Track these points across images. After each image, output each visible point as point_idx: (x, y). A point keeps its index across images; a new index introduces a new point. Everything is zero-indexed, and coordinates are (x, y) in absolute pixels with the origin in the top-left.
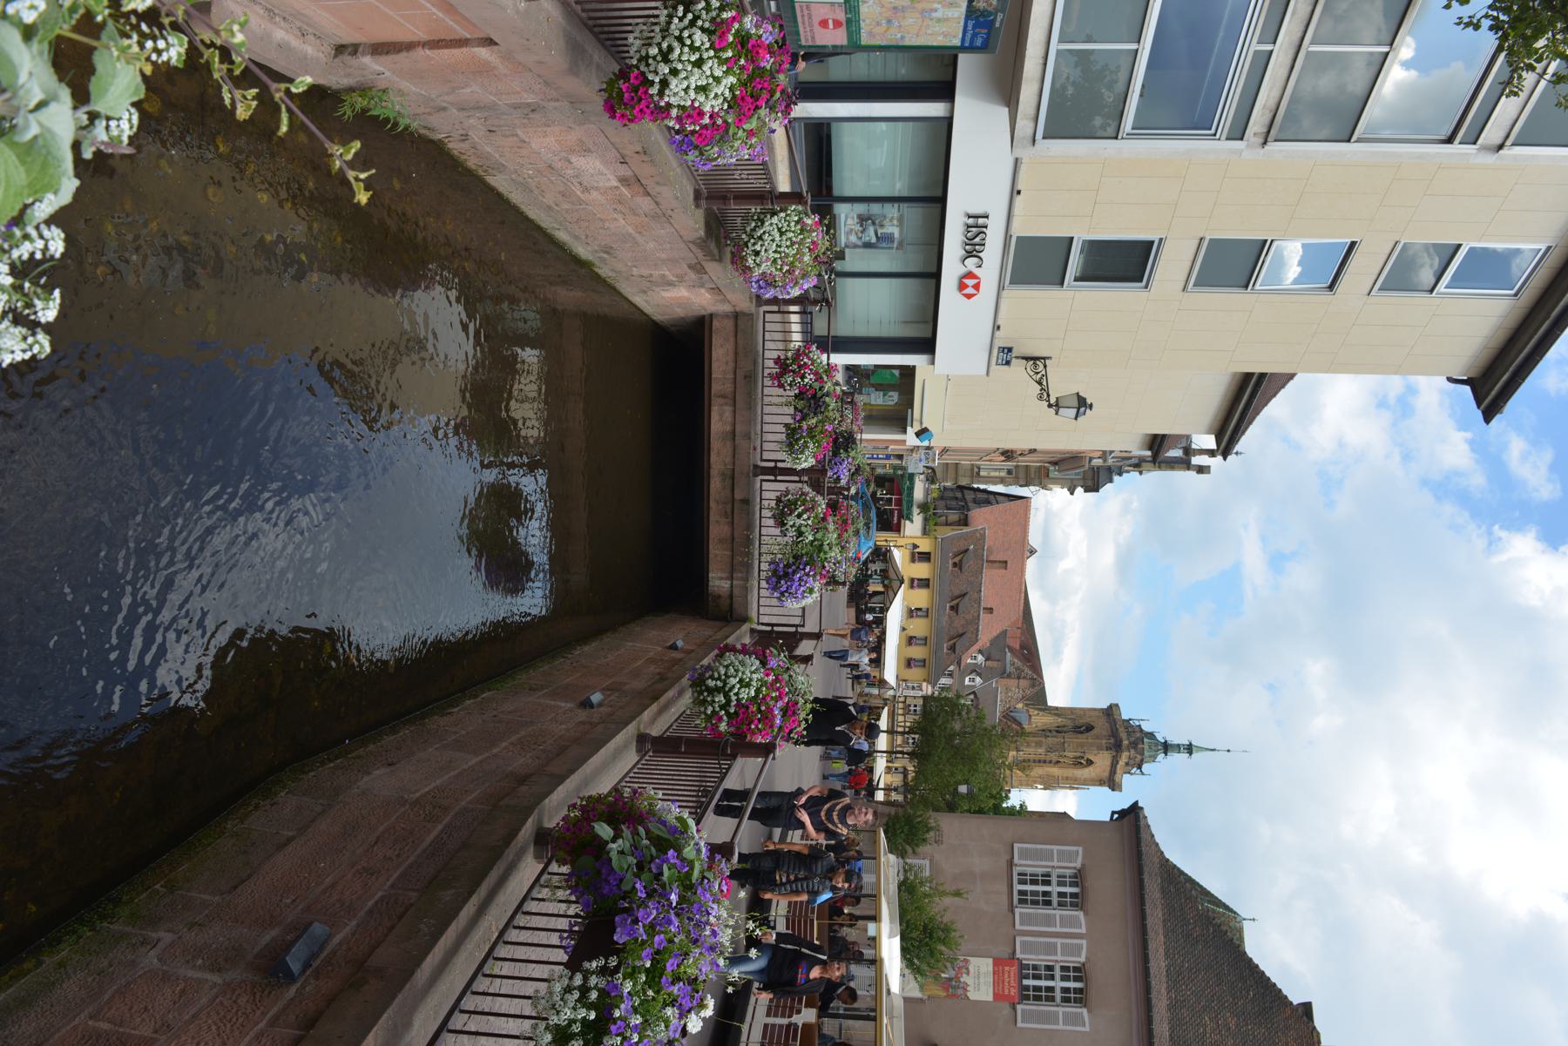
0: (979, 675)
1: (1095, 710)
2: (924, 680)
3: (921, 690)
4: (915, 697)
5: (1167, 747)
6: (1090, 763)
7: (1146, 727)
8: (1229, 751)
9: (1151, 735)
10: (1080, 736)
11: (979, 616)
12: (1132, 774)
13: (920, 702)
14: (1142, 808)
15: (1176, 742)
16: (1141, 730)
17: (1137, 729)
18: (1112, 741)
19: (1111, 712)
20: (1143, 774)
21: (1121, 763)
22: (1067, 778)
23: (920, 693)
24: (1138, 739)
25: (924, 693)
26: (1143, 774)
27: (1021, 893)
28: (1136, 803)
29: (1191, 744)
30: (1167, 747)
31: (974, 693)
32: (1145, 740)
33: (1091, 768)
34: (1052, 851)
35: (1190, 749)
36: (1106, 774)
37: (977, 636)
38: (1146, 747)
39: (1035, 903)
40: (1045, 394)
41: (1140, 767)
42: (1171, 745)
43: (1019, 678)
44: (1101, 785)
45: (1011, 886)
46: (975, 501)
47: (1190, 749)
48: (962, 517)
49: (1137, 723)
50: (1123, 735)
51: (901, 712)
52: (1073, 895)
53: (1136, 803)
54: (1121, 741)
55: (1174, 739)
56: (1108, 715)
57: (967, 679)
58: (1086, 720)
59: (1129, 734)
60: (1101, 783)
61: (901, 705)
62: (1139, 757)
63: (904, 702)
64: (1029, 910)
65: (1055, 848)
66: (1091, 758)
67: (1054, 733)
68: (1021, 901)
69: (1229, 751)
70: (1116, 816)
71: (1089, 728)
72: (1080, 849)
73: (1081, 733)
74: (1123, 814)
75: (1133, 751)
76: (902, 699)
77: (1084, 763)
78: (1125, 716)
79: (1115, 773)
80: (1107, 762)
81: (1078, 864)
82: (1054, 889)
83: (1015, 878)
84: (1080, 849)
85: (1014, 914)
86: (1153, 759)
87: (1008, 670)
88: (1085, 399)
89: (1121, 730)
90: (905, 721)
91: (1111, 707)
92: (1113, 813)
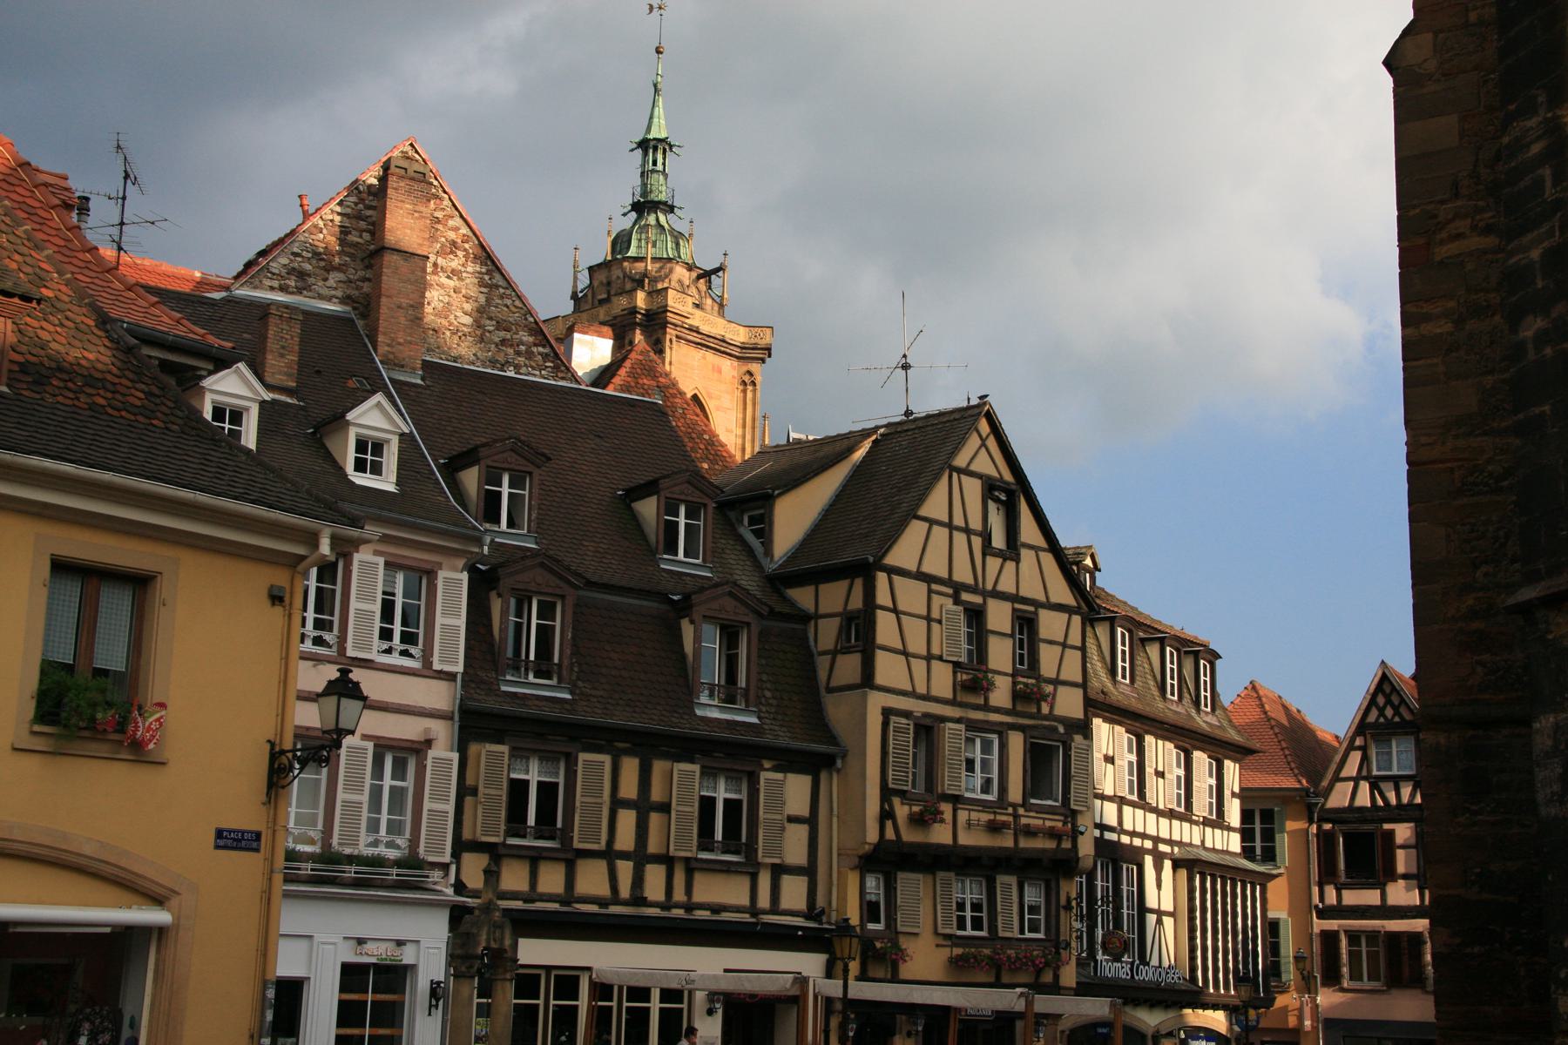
0: (337, 421)
3: (419, 748)
4: (465, 791)
9: (621, 242)
15: (639, 182)
16: (605, 265)
17: (601, 276)
21: (697, 319)
23: (443, 752)
25: (442, 733)
32: (632, 252)
42: (644, 193)
49: (584, 280)
51: (552, 880)
61: (514, 878)
63: (496, 854)
90: (610, 855)
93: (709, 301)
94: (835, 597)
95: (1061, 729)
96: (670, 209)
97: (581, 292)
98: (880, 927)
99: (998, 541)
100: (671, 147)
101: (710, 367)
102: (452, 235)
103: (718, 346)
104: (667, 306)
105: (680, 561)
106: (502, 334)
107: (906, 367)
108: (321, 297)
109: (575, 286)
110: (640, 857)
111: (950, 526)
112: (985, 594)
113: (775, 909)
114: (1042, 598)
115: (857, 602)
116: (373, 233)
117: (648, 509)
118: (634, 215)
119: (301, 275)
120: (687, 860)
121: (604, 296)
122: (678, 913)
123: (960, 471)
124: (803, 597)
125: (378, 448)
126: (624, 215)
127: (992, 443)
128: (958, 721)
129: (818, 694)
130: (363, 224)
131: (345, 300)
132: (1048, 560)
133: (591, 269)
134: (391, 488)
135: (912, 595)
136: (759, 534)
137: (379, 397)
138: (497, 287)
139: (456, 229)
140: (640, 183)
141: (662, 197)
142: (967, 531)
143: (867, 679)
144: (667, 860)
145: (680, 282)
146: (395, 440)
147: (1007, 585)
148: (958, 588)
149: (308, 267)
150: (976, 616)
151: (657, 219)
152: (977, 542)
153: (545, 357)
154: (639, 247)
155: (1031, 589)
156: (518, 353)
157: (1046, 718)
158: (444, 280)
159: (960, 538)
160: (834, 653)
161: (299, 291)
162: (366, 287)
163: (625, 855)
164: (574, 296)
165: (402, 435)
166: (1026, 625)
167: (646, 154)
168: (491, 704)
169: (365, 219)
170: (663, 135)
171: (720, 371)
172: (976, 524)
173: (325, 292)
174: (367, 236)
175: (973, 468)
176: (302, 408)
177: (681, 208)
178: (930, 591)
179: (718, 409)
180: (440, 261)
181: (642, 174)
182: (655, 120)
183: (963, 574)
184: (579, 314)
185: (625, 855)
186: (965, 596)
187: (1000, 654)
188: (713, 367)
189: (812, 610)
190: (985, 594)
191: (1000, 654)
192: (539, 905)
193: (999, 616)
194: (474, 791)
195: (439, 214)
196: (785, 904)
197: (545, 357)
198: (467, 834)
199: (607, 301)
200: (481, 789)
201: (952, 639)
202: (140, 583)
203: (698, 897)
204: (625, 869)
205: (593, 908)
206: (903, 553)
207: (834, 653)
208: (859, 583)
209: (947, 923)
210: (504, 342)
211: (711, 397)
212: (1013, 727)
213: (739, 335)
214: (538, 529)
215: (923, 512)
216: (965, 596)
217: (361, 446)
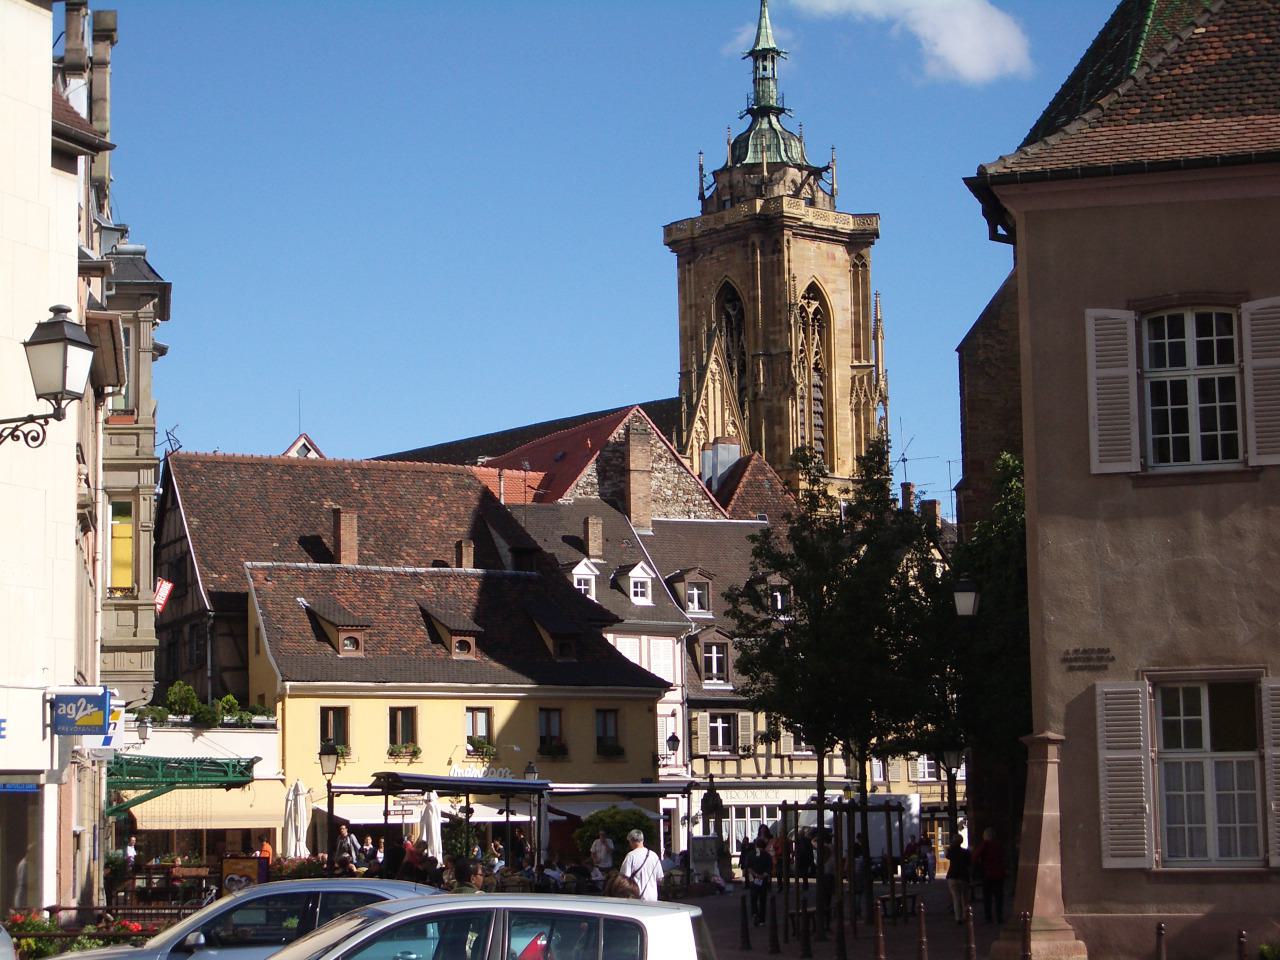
1: (682, 283)
6: (814, 292)
7: (720, 157)
9: (739, 147)
10: (749, 317)
13: (703, 717)
14: (982, 170)
15: (750, 88)
16: (725, 169)
17: (725, 179)
19: (684, 243)
21: (810, 216)
22: (857, 346)
27: (1209, 453)
28: (967, 181)
31: (670, 582)
32: (748, 160)
33: (828, 289)
34: (1101, 380)
38: (766, 158)
39: (1230, 417)
40: (27, 428)
41: (816, 173)
42: (757, 100)
45: (1196, 477)
49: (710, 179)
52: (1203, 326)
53: (967, 181)
54: (755, 217)
57: (638, 601)
59: (735, 200)
61: (715, 768)
62: (793, 173)
64: (1249, 430)
65: (1093, 374)
66: (801, 289)
67: (747, 380)
68: (1231, 452)
70: (1001, 231)
72: (1091, 313)
73: (741, 313)
74: (997, 216)
75: (779, 190)
76: (698, 765)
78: (694, 210)
79: (834, 232)
81: (1128, 317)
82: (1192, 373)
83: (1173, 467)
84: (1091, 313)
85: (1261, 468)
88: (41, 326)
91: (672, 244)
92: (994, 236)
93: (820, 194)
96: (779, 111)
97: (708, 189)
100: (778, 53)
101: (825, 255)
102: (659, 451)
103: (831, 235)
104: (783, 212)
106: (686, 497)
107: (904, 460)
109: (701, 187)
110: (768, 756)
113: (831, 774)
118: (749, 118)
120: (789, 756)
121: (728, 197)
122: (787, 779)
126: (741, 118)
130: (618, 454)
133: (715, 173)
134: (651, 604)
137: (642, 564)
138: (682, 473)
139: (661, 448)
140: (752, 91)
141: (773, 102)
144: (781, 757)
145: (793, 181)
146: (650, 584)
151: (770, 123)
154: (755, 152)
156: (694, 505)
158: (657, 474)
163: (762, 756)
164: (701, 196)
165: (652, 578)
167: (756, 60)
169: (618, 451)
170: (772, 45)
171: (834, 258)
177: (790, 110)
180: (655, 465)
181: (754, 81)
182: (763, 30)
184: (707, 217)
185: (762, 756)
188: (828, 255)
192: (727, 780)
194: (696, 733)
196: (835, 772)
197: (708, 504)
198: (694, 752)
200: (699, 733)
202: (615, 711)
203: (795, 772)
204: (762, 761)
205: (750, 779)
211: (826, 282)
213: (848, 225)
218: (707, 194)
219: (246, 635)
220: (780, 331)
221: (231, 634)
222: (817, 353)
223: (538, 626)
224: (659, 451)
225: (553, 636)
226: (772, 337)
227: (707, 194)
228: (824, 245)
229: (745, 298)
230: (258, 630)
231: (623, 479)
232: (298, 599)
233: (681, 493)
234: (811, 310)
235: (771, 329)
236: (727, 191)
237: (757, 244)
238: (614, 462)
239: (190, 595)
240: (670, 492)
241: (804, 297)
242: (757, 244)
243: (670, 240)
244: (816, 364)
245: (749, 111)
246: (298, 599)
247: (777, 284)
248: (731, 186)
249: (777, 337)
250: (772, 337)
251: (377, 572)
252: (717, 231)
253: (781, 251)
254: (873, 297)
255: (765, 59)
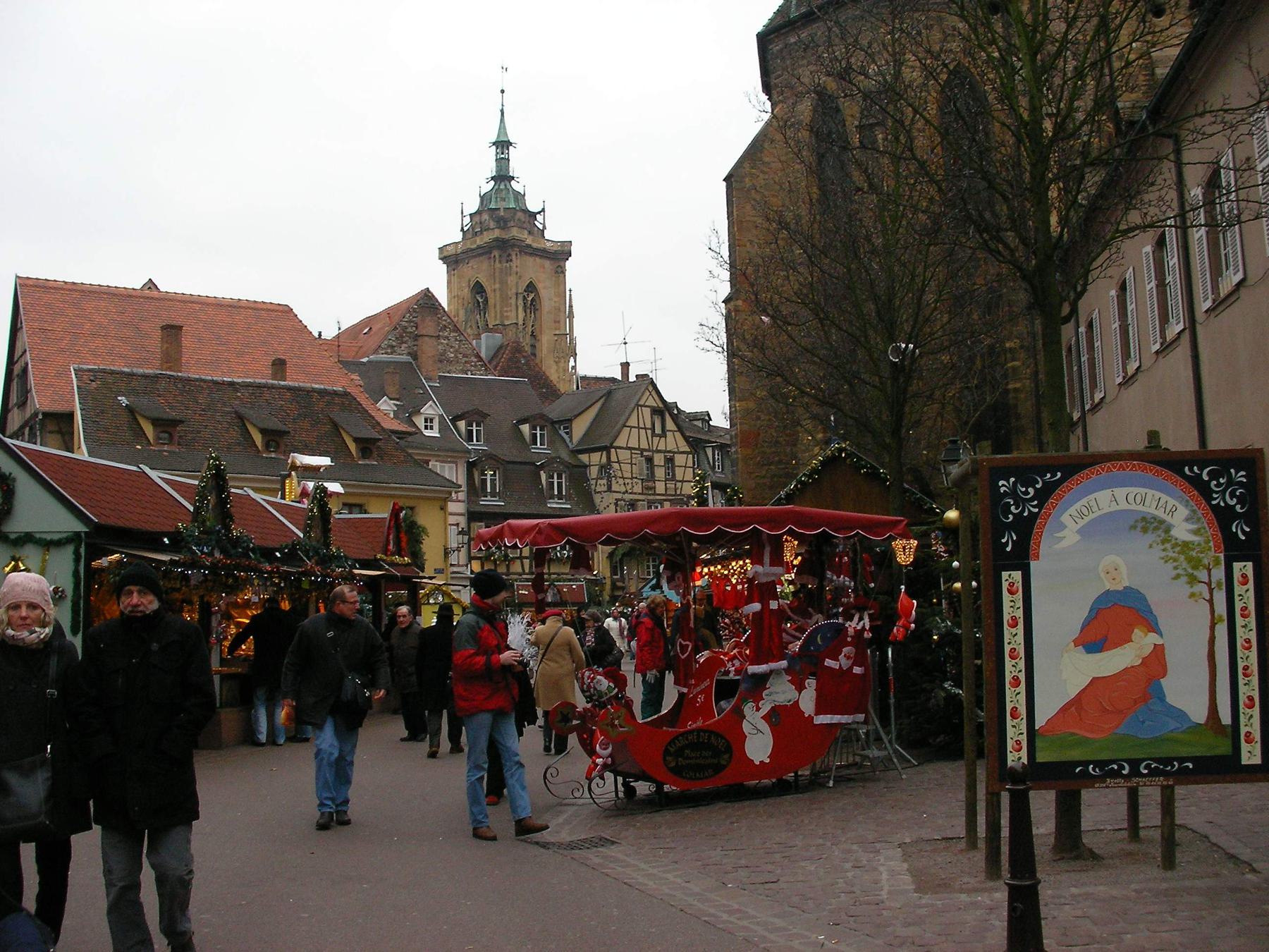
1: (449, 282)
2: (443, 508)
5: (502, 177)
6: (531, 287)
7: (473, 205)
8: (503, 91)
10: (491, 302)
11: (289, 389)
12: (544, 227)
15: (494, 164)
16: (478, 212)
17: (477, 219)
18: (496, 253)
20: (543, 210)
24: (491, 217)
26: (543, 210)
29: (494, 144)
30: (502, 177)
31: (455, 420)
32: (492, 206)
33: (540, 286)
35: (503, 145)
36: (547, 263)
37: (335, 393)
38: (502, 205)
41: (533, 215)
43: (416, 337)
44: (563, 272)
46: (22, 404)
47: (503, 145)
48: (51, 426)
49: (467, 220)
50: (487, 237)
54: (496, 240)
55: (490, 168)
56: (457, 262)
57: (427, 433)
58: (466, 292)
60: (561, 271)
62: (520, 215)
69: (503, 91)
71: (478, 289)
73: (486, 300)
77: (532, 296)
78: (458, 237)
80: (529, 261)
86: (520, 197)
87: (405, 358)
89: (479, 241)
93: (536, 229)
94: (596, 458)
95: (685, 499)
98: (618, 577)
99: (658, 430)
102: (444, 323)
105: (540, 449)
107: (625, 343)
108: (400, 354)
109: (462, 224)
111: (639, 428)
112: (653, 451)
114: (676, 450)
115: (604, 460)
116: (417, 328)
117: (525, 428)
118: (492, 183)
119: (393, 347)
123: (641, 406)
124: (584, 458)
125: (431, 421)
127: (653, 393)
128: (644, 501)
129: (591, 495)
131: (409, 354)
132: (678, 435)
133: (470, 215)
135: (623, 455)
136: (567, 433)
139: (445, 321)
142: (645, 428)
143: (609, 489)
145: (519, 220)
146: (437, 418)
147: (661, 447)
148: (643, 450)
149: (394, 343)
150: (650, 460)
151: (505, 185)
152: (649, 432)
153: (482, 366)
154: (496, 202)
155: (671, 446)
156: (472, 366)
157: (679, 495)
159: (642, 432)
160: (597, 479)
161: (392, 353)
162: (415, 348)
163: (526, 558)
164: (462, 229)
166: (670, 461)
167: (497, 148)
168: (477, 509)
169: (413, 322)
171: (544, 268)
172: (649, 425)
173: (401, 352)
174: (414, 329)
175: (646, 404)
176: (402, 406)
178: (632, 453)
179: (544, 288)
183: (644, 445)
185: (526, 558)
186: (645, 454)
187: (660, 473)
189: (588, 463)
190: (653, 451)
191: (660, 473)
193: (659, 459)
195: (439, 316)
199: (481, 232)
201: (641, 469)
206: (621, 442)
207: (597, 479)
208: (604, 453)
209: (643, 574)
210: (466, 362)
211: (539, 282)
212: (666, 500)
214: (487, 442)
215: (627, 424)
216: (645, 454)
217: (426, 421)
218: (465, 229)
219: (73, 433)
220: (511, 311)
221: (60, 432)
222: (533, 326)
223: (342, 432)
224: (444, 323)
225: (356, 440)
226: (505, 314)
227: (465, 229)
228: (538, 260)
229: (488, 290)
230: (78, 422)
231: (416, 343)
232: (119, 398)
233: (460, 356)
234: (530, 299)
235: (505, 309)
236: (478, 226)
237: (497, 256)
238: (409, 330)
239: (29, 401)
240: (453, 355)
241: (525, 291)
242: (497, 256)
243: (442, 256)
244: (533, 332)
245: (492, 178)
246: (119, 398)
247: (509, 282)
248: (481, 223)
249: (509, 314)
250: (505, 314)
251: (197, 380)
252: (473, 250)
253: (511, 260)
254: (568, 293)
255: (503, 147)
